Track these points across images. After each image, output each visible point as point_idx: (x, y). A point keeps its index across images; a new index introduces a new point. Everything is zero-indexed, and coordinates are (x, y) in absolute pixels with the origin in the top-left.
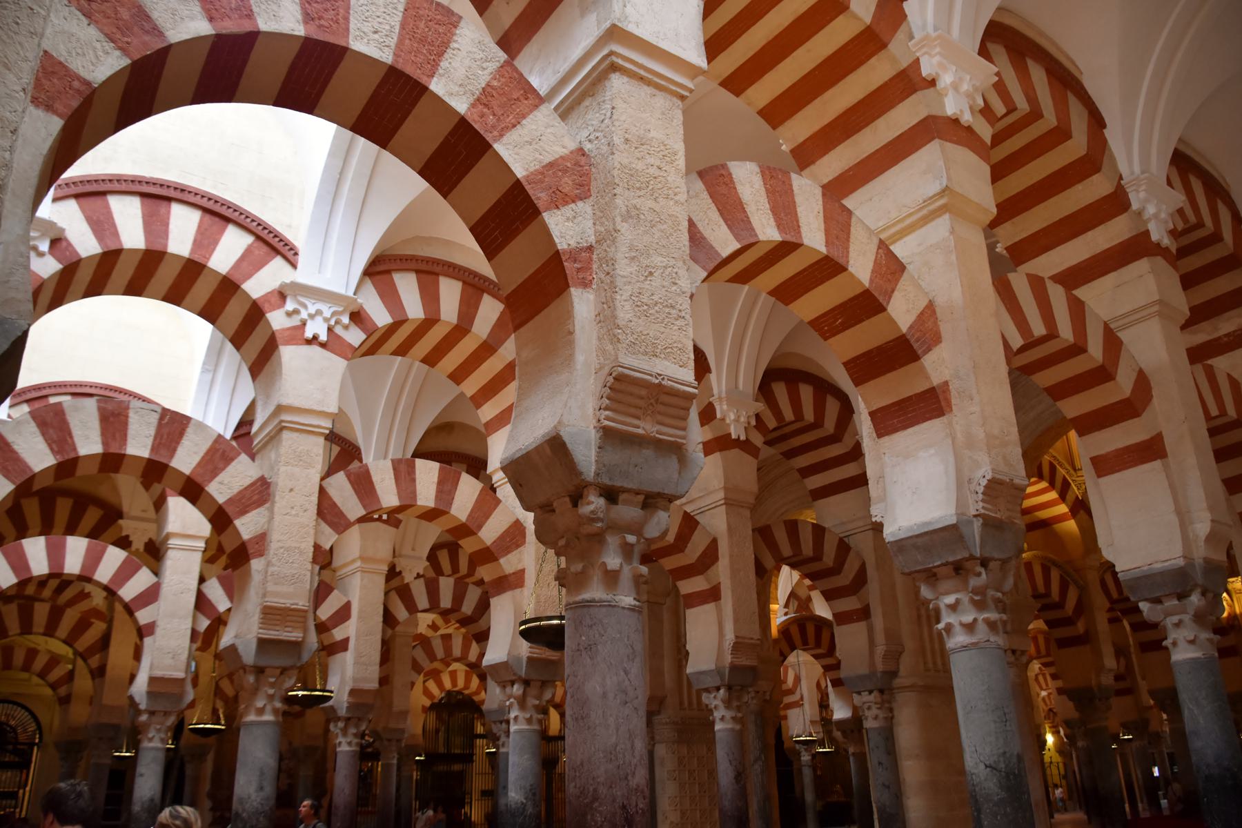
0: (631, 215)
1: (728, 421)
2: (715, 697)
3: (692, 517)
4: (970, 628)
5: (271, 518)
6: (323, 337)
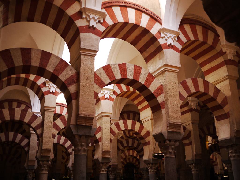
0: (170, 96)
1: (192, 105)
2: (192, 166)
3: (184, 126)
4: (234, 156)
5: (102, 134)
6: (108, 98)
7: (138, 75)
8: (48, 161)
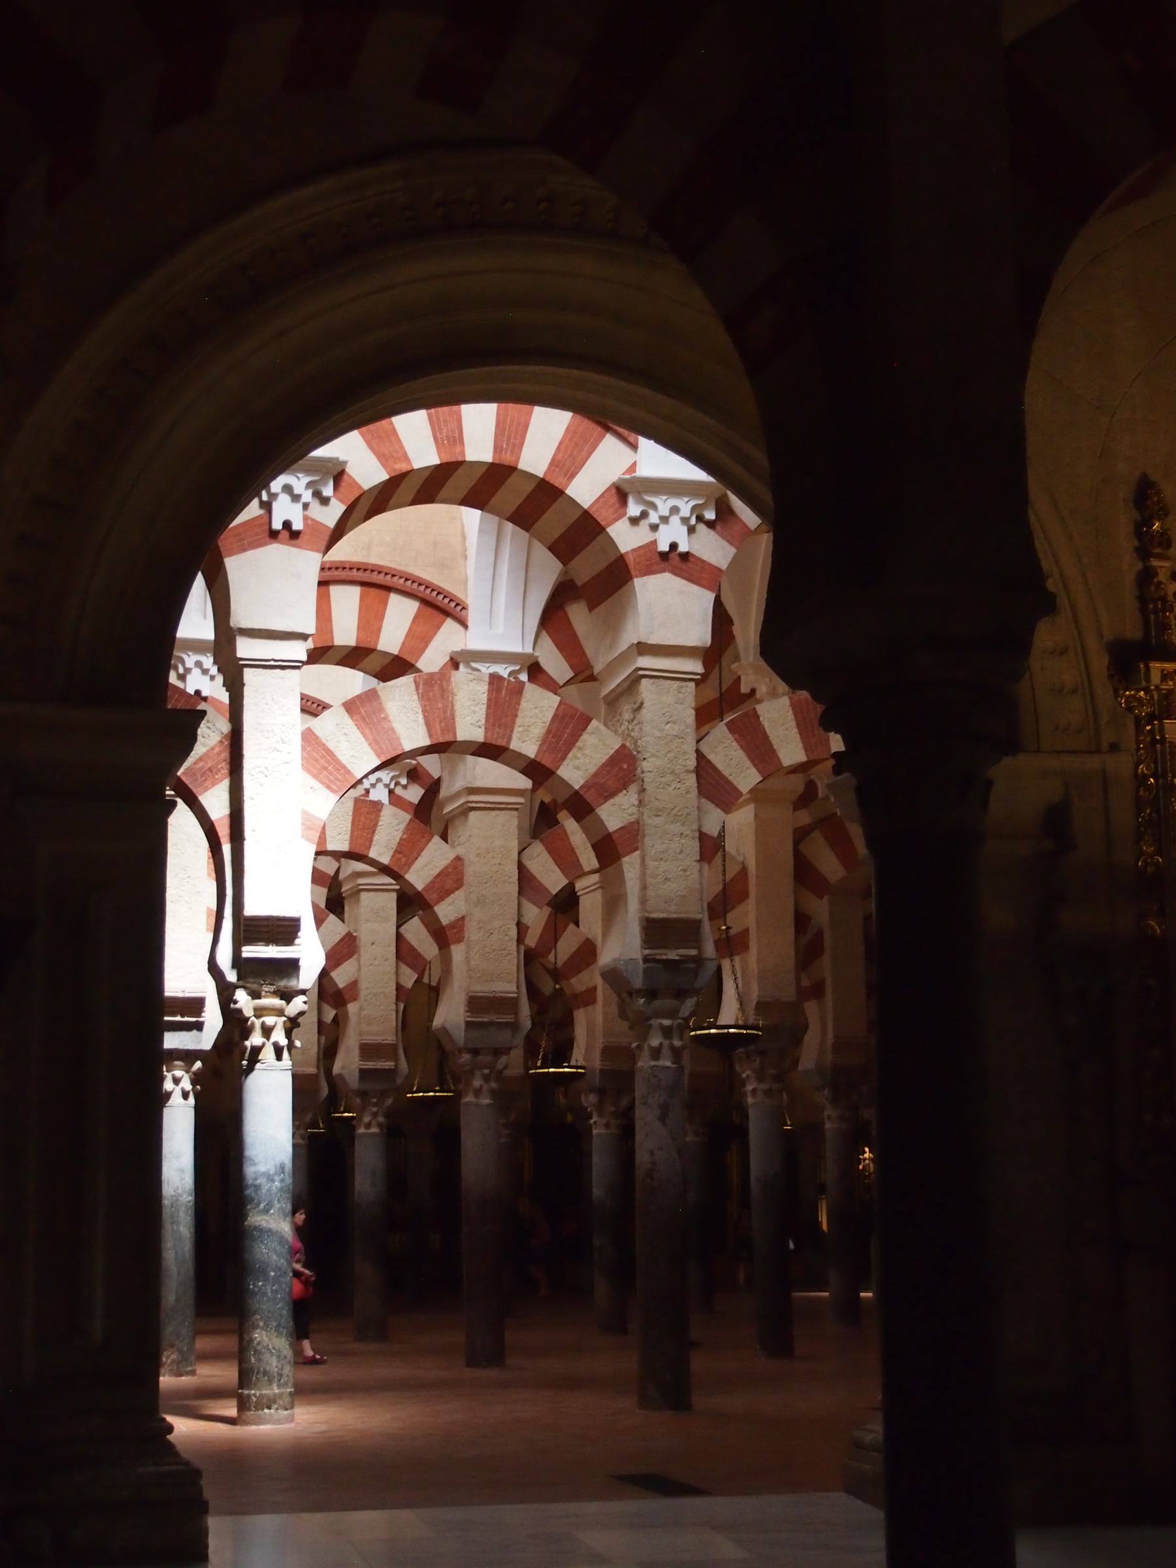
7: (368, 833)
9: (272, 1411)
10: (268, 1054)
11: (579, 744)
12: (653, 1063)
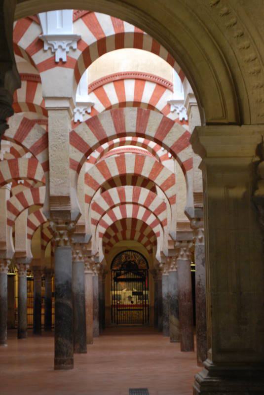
8: (89, 257)
9: (64, 365)
10: (62, 244)
11: (171, 131)
12: (200, 244)
